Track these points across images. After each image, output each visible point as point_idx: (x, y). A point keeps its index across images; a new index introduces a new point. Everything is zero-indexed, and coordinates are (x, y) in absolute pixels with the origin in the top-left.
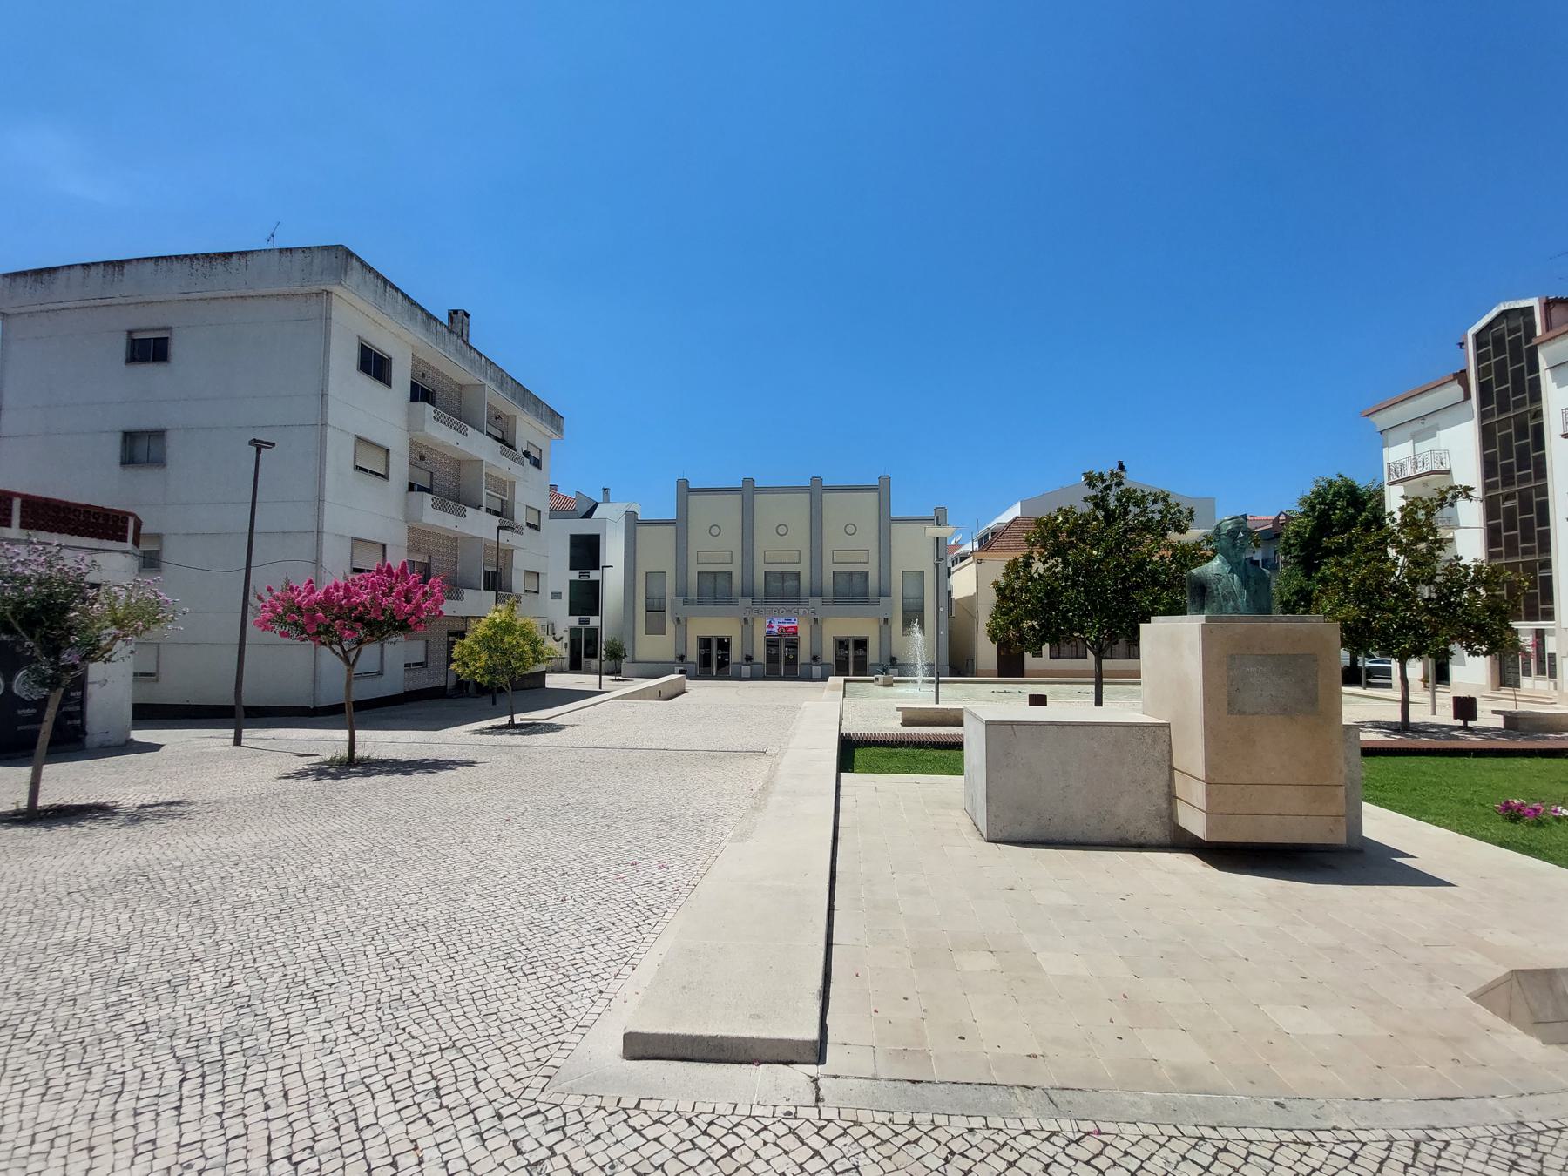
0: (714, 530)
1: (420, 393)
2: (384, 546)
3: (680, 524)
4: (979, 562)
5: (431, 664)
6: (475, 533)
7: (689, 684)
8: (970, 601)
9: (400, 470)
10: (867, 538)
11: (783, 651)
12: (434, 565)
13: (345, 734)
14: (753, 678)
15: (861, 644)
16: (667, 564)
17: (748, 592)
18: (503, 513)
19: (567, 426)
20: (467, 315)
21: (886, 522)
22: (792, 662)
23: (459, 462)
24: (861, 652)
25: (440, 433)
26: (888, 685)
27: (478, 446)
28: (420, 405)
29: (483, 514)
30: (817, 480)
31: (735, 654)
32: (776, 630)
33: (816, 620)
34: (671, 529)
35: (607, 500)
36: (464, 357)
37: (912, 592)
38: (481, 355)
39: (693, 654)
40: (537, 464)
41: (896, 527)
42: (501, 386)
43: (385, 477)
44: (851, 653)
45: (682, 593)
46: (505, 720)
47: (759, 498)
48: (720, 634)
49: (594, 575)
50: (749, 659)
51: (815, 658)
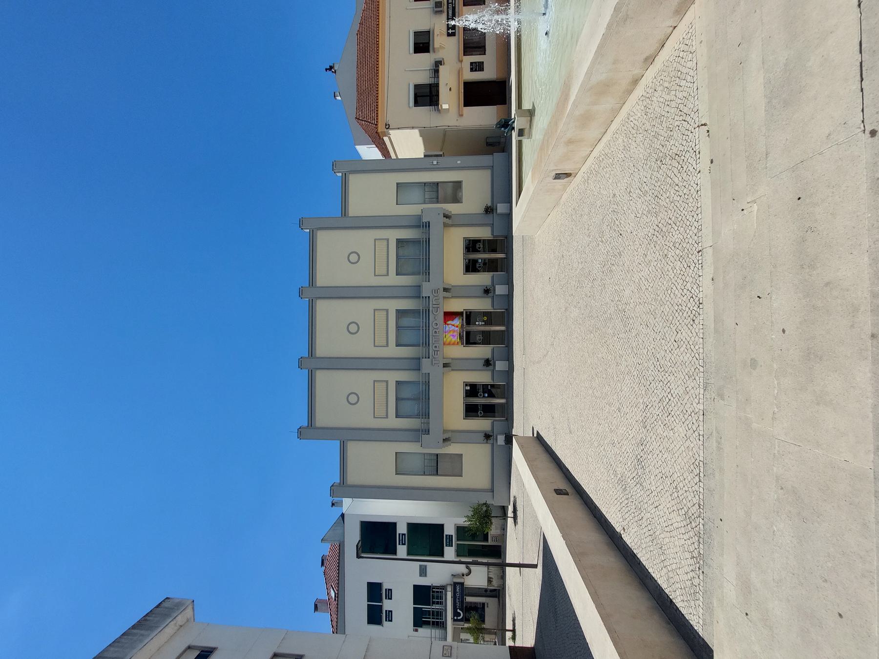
3: (345, 436)
4: (388, 126)
8: (427, 135)
11: (479, 326)
14: (509, 357)
17: (415, 364)
22: (489, 317)
31: (482, 377)
39: (482, 424)
44: (481, 256)
49: (402, 529)
50: (488, 363)
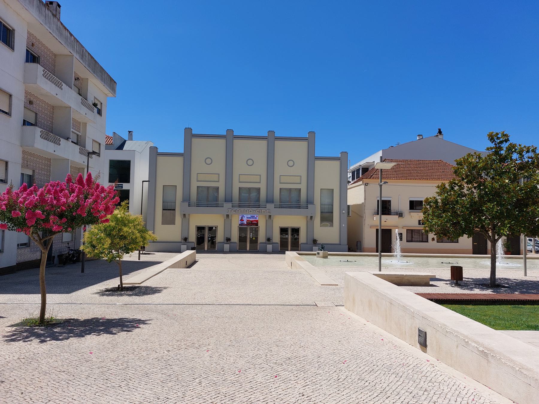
0: (250, 162)
1: (32, 58)
2: (7, 163)
3: (186, 156)
4: (366, 185)
5: (32, 244)
6: (65, 156)
7: (199, 256)
8: (360, 207)
9: (19, 110)
10: (301, 169)
11: (249, 235)
12: (36, 176)
13: (37, 298)
14: (231, 251)
15: (296, 231)
16: (178, 182)
17: (228, 199)
18: (79, 142)
19: (118, 88)
20: (59, 6)
21: (312, 159)
22: (254, 241)
23: (53, 107)
24: (243, 235)
25: (46, 87)
26: (325, 257)
27: (68, 97)
28: (33, 66)
29: (69, 143)
30: (230, 131)
31: (220, 237)
32: (245, 222)
33: (228, 216)
34: (180, 159)
35: (131, 138)
36: (61, 34)
37: (327, 201)
38: (71, 35)
39: (193, 237)
40: (99, 112)
41: (317, 163)
42: (82, 57)
43: (8, 114)
44: (289, 237)
45: (187, 199)
46: (114, 283)
47: (236, 142)
48: (210, 225)
49: (125, 186)
50: (228, 240)
51: (269, 240)
